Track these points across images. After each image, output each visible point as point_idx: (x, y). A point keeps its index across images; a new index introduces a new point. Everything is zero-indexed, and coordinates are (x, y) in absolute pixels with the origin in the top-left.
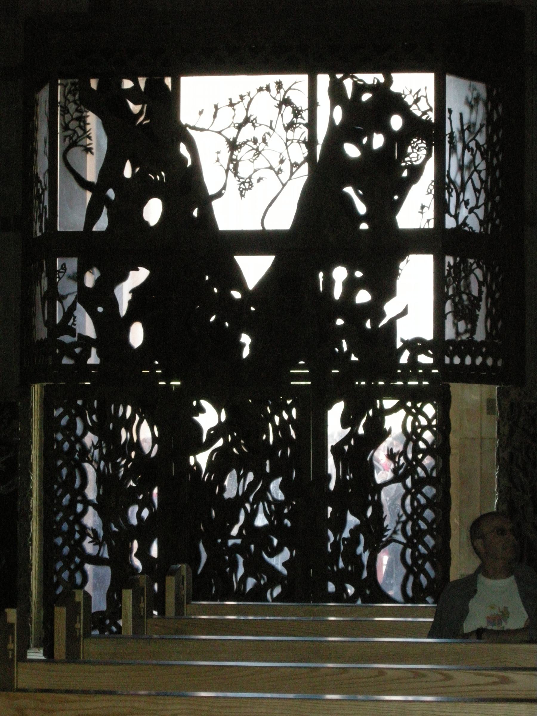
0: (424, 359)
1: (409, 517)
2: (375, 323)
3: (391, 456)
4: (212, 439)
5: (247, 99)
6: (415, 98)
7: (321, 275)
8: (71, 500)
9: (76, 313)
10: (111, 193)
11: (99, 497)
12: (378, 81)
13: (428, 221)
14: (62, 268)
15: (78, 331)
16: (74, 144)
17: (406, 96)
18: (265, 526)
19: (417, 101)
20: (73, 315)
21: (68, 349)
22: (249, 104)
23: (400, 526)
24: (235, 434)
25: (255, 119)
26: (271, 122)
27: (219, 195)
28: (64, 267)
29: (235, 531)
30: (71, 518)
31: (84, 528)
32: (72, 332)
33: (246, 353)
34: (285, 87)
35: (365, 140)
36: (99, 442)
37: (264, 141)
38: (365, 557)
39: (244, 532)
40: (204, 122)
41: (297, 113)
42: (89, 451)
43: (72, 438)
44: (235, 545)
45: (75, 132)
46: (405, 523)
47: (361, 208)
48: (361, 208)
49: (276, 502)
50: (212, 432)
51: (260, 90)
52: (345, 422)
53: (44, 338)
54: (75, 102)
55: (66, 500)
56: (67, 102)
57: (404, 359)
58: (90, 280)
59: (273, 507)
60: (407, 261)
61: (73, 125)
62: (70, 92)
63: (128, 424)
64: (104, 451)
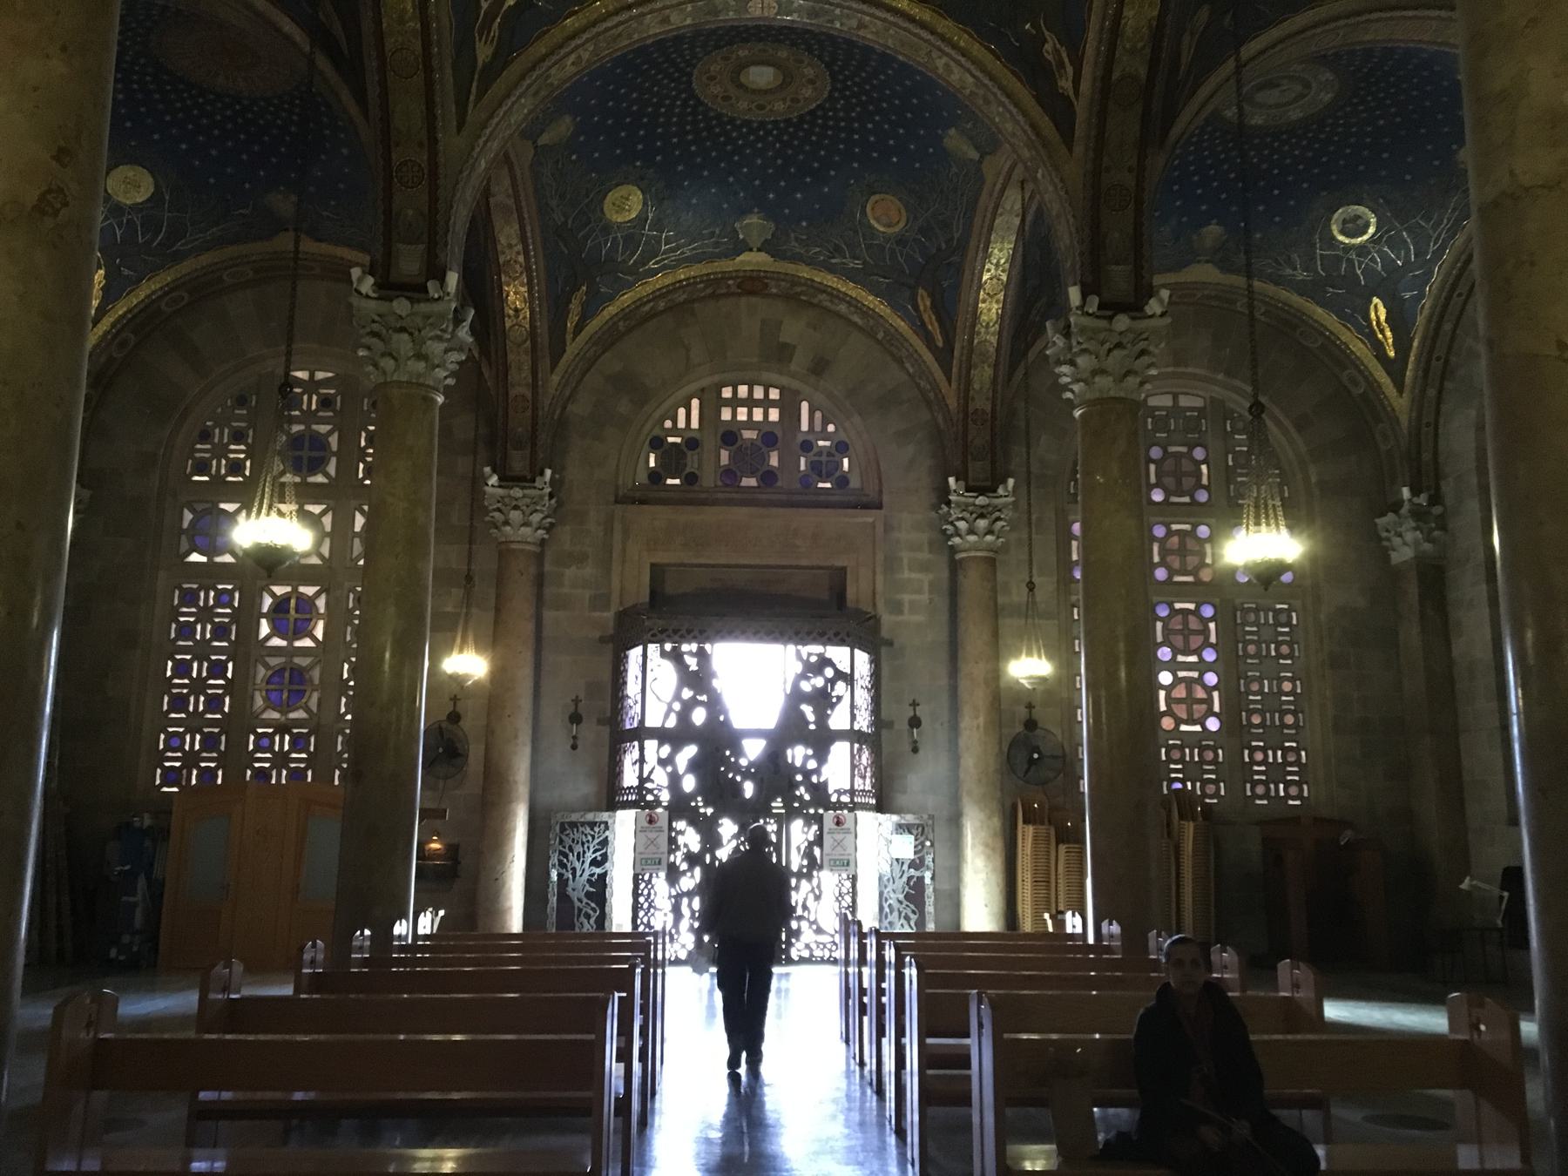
4: (729, 841)
15: (656, 782)
21: (650, 791)
32: (652, 781)
48: (811, 717)
63: (682, 833)
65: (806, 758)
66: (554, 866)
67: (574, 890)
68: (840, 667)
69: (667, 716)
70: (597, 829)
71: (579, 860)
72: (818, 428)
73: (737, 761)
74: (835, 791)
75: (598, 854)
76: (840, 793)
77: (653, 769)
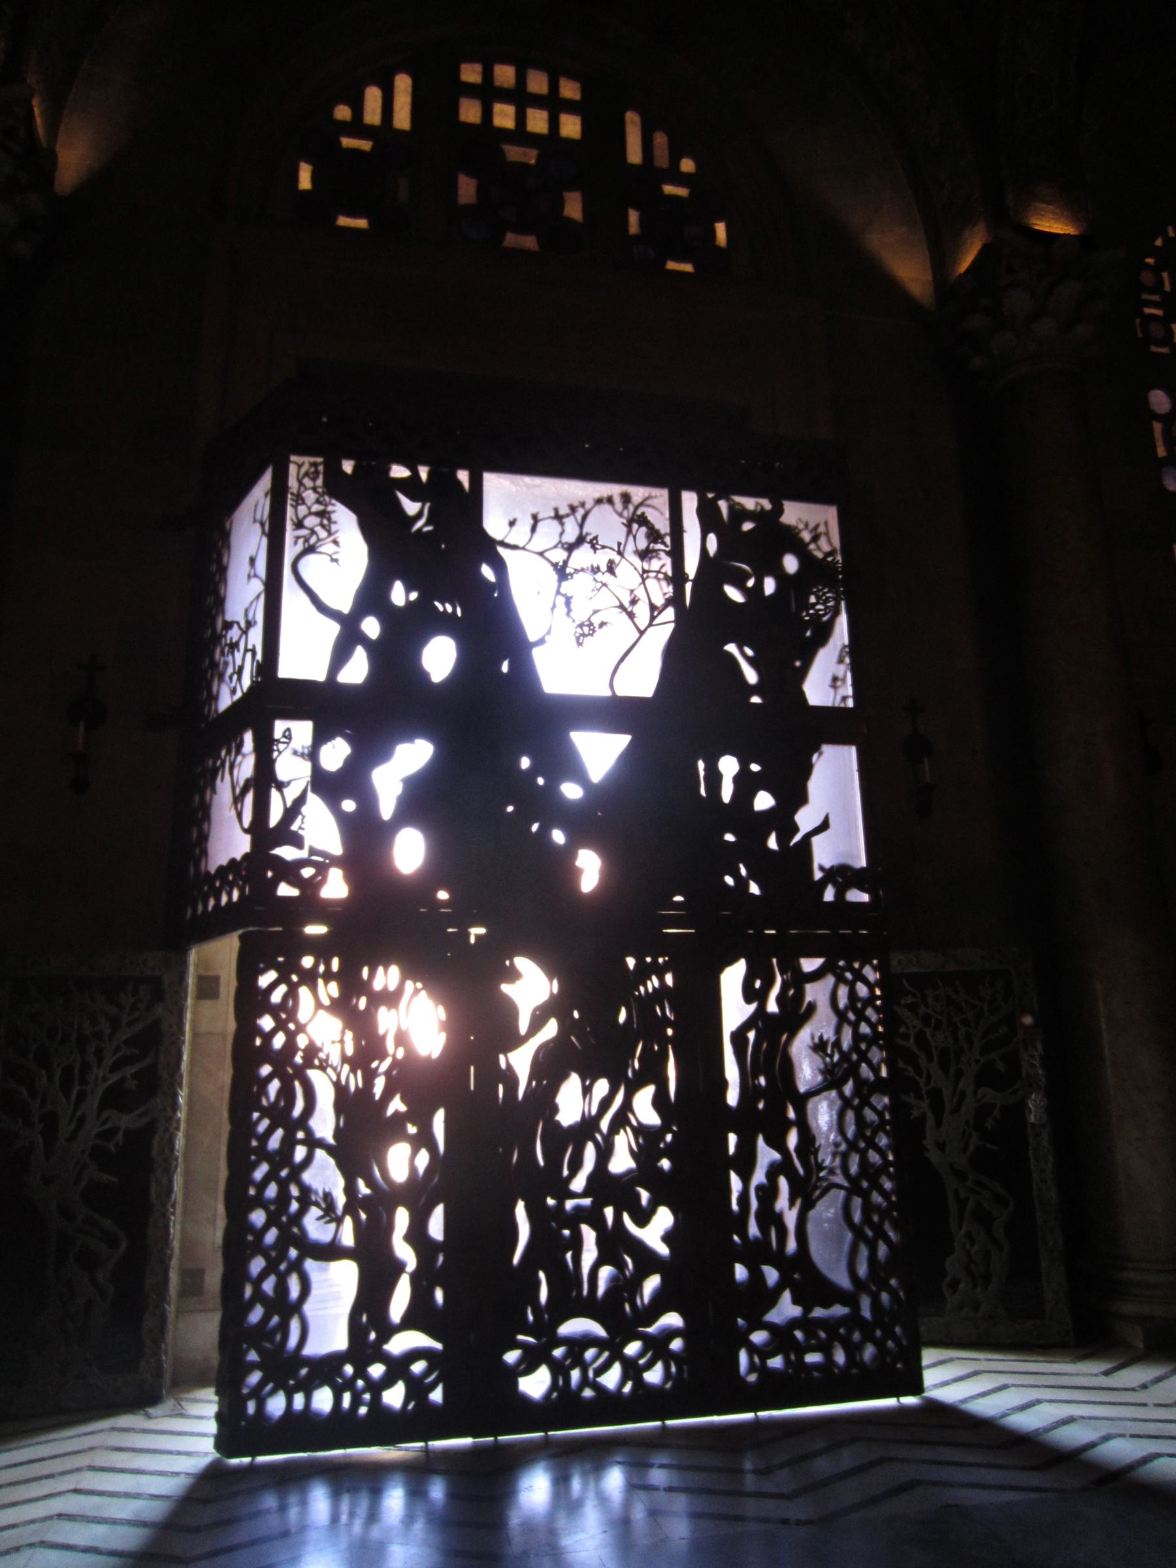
1: (852, 1146)
2: (783, 840)
3: (819, 1047)
4: (537, 1024)
5: (580, 512)
6: (813, 534)
7: (701, 765)
11: (338, 1133)
12: (762, 508)
13: (844, 698)
14: (284, 736)
16: (310, 550)
17: (800, 531)
18: (629, 1172)
19: (815, 539)
21: (289, 872)
22: (584, 518)
23: (838, 1161)
25: (596, 538)
26: (619, 544)
27: (541, 642)
28: (288, 735)
30: (284, 1173)
31: (306, 1191)
35: (751, 583)
38: (791, 1219)
40: (519, 535)
41: (654, 535)
43: (292, 1026)
44: (578, 1208)
45: (313, 532)
46: (845, 1157)
47: (751, 676)
48: (751, 676)
49: (641, 1130)
51: (599, 501)
52: (749, 994)
54: (314, 489)
55: (275, 1142)
56: (302, 489)
57: (829, 895)
60: (820, 754)
61: (311, 521)
62: (307, 474)
63: (391, 998)
65: (746, 785)
68: (819, 550)
69: (341, 655)
71: (67, 1092)
72: (662, 159)
73: (552, 789)
75: (130, 1070)
76: (842, 875)
77: (301, 800)
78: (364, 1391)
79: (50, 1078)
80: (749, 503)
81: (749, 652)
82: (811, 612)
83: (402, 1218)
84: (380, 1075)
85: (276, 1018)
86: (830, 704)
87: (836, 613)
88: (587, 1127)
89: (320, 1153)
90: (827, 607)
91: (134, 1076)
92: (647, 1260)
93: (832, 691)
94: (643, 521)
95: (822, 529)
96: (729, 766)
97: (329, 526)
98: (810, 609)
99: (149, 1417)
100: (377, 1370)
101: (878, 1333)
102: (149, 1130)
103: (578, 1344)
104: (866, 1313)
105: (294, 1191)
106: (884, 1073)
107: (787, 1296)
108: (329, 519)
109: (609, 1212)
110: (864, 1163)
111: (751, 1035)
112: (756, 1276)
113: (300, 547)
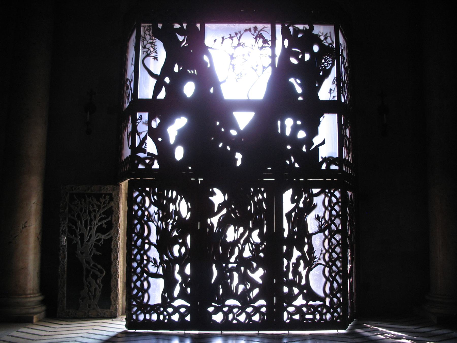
0: (333, 167)
3: (318, 218)
4: (220, 209)
5: (239, 35)
6: (325, 37)
8: (142, 243)
9: (146, 141)
10: (167, 80)
11: (157, 241)
12: (306, 28)
13: (334, 97)
14: (140, 118)
15: (147, 151)
16: (148, 55)
17: (320, 36)
19: (326, 38)
20: (145, 142)
21: (142, 161)
23: (322, 256)
24: (233, 207)
25: (244, 44)
27: (224, 81)
28: (141, 117)
29: (233, 260)
30: (142, 252)
31: (148, 257)
32: (144, 151)
33: (239, 163)
34: (259, 29)
35: (300, 56)
36: (158, 210)
37: (249, 54)
38: (304, 273)
39: (238, 260)
41: (265, 41)
42: (153, 216)
43: (143, 209)
44: (233, 267)
45: (149, 49)
48: (299, 90)
49: (254, 244)
50: (220, 206)
51: (246, 30)
52: (293, 201)
53: (128, 156)
54: (149, 35)
56: (145, 35)
57: (324, 167)
58: (154, 124)
59: (254, 246)
60: (324, 117)
61: (148, 46)
62: (147, 30)
63: (174, 201)
64: (161, 216)
65: (295, 129)
66: (64, 232)
67: (82, 253)
69: (157, 90)
70: (102, 200)
71: (86, 227)
73: (227, 131)
74: (325, 160)
75: (104, 222)
76: (329, 160)
78: (166, 316)
79: (81, 223)
80: (301, 27)
81: (299, 81)
82: (322, 66)
83: (177, 267)
84: (170, 224)
85: (138, 206)
86: (329, 99)
87: (333, 65)
88: (235, 243)
89: (152, 247)
90: (328, 64)
91: (105, 223)
92: (254, 284)
93: (329, 94)
94: (261, 36)
95: (328, 35)
96: (289, 122)
97: (154, 47)
98: (322, 65)
99: (113, 321)
100: (170, 310)
101: (332, 310)
102: (110, 240)
103: (231, 308)
104: (328, 303)
105: (145, 257)
106: (340, 228)
107: (301, 297)
108: (154, 45)
109: (242, 269)
110: (330, 256)
111: (293, 214)
112: (291, 291)
113: (145, 55)
